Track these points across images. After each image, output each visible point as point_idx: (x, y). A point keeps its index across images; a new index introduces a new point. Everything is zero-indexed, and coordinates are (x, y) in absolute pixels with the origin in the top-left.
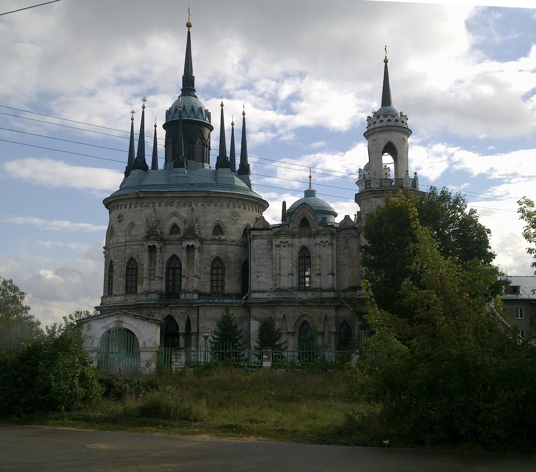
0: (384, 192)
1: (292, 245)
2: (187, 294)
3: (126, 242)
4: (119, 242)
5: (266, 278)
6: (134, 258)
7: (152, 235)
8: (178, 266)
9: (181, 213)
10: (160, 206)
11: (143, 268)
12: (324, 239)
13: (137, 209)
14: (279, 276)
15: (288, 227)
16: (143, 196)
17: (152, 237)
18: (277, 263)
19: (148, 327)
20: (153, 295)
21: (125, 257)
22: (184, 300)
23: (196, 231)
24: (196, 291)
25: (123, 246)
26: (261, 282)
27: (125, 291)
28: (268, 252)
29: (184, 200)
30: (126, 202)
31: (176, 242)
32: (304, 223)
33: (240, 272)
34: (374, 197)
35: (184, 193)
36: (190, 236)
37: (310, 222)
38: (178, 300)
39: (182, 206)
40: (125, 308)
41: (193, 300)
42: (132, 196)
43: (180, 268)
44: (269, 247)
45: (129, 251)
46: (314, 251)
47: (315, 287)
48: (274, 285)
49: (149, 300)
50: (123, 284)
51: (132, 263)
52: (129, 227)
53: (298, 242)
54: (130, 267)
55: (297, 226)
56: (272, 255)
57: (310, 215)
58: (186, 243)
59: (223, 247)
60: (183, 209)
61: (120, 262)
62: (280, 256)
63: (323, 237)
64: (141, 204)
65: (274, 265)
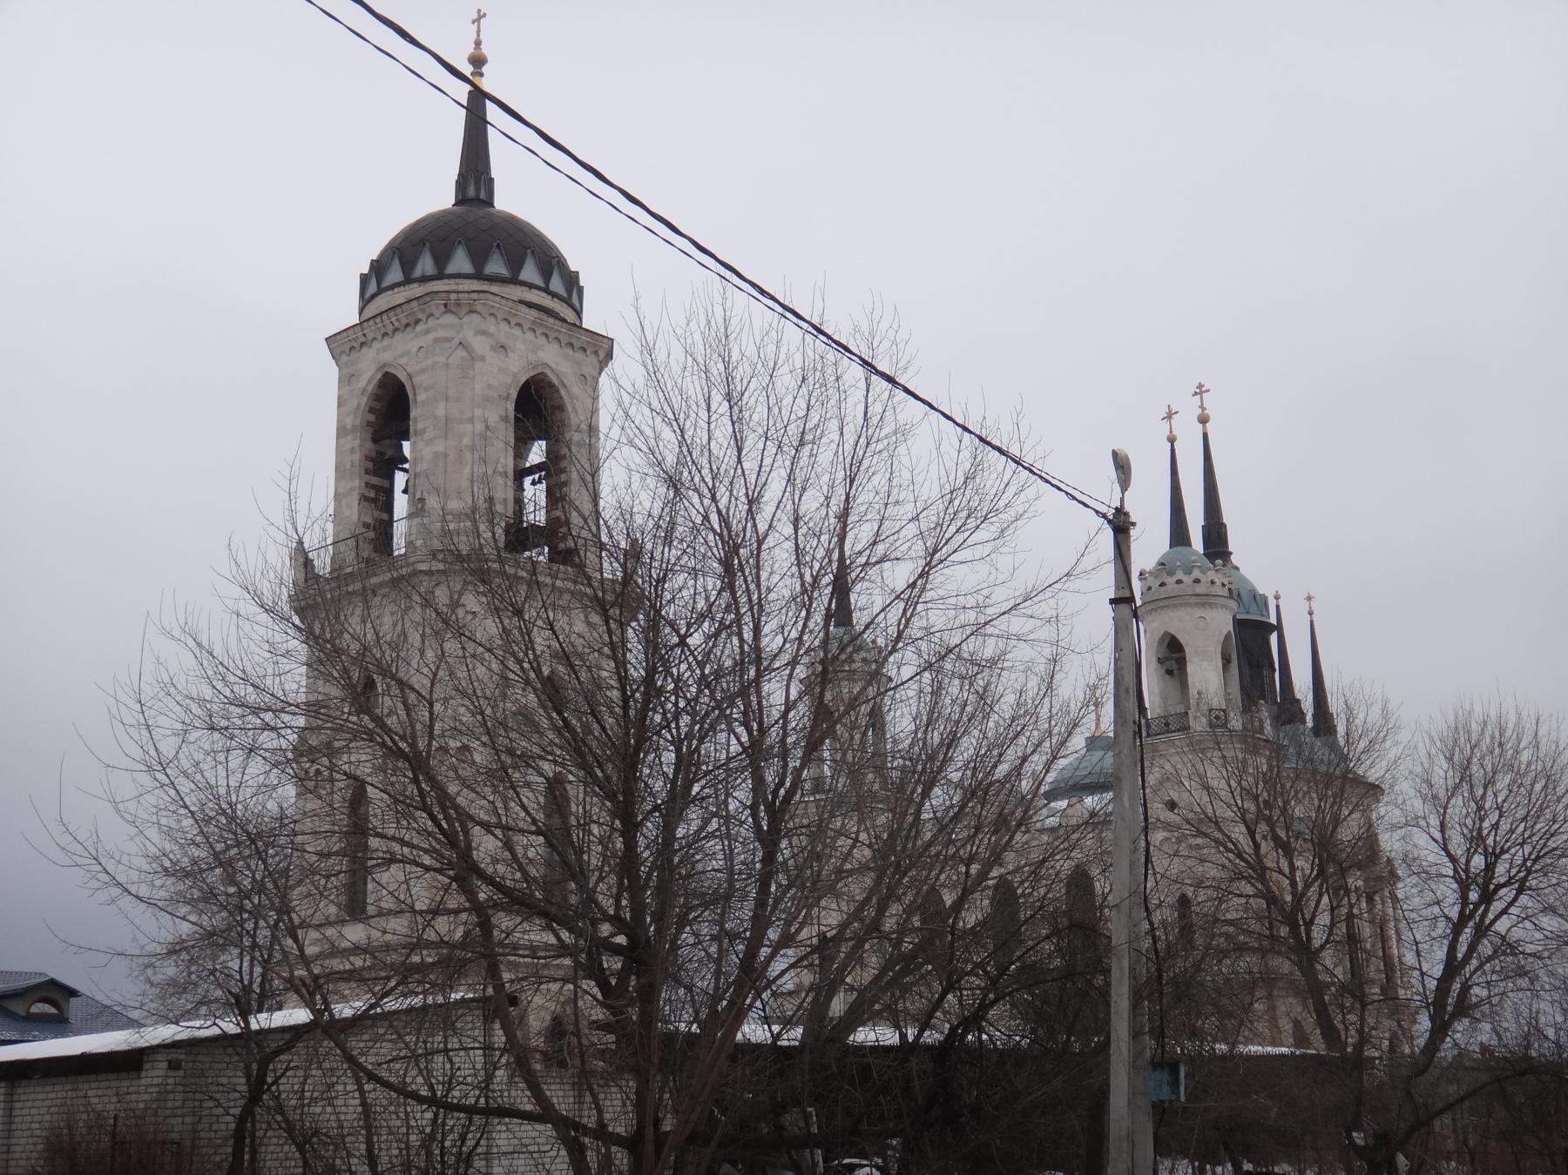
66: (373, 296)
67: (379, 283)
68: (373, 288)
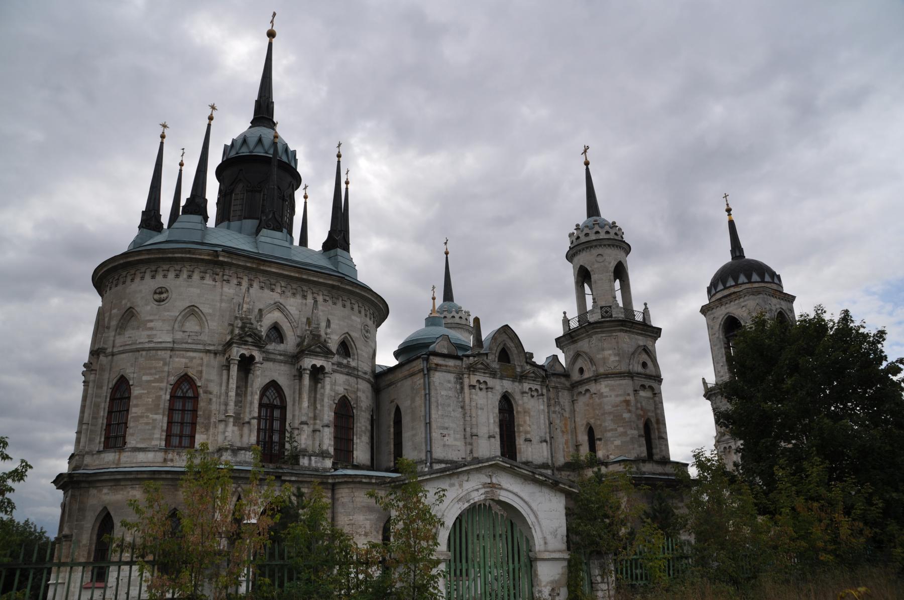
0: (634, 325)
1: (492, 388)
2: (313, 458)
3: (174, 342)
4: (155, 340)
5: (456, 439)
6: (191, 375)
7: (250, 336)
8: (277, 402)
9: (287, 307)
10: (251, 285)
11: (211, 400)
12: (534, 387)
13: (203, 284)
14: (476, 437)
15: (487, 358)
16: (226, 260)
17: (250, 339)
18: (474, 415)
19: (550, 500)
20: (248, 453)
21: (169, 372)
22: (308, 469)
23: (328, 343)
24: (323, 455)
25: (165, 349)
26: (448, 445)
27: (166, 441)
28: (457, 396)
29: (295, 286)
30: (180, 266)
31: (279, 357)
32: (504, 356)
33: (369, 427)
34: (621, 331)
35: (298, 272)
36: (318, 350)
37: (511, 359)
38: (296, 467)
39: (289, 294)
40: (169, 476)
41: (325, 470)
42: (202, 257)
43: (283, 408)
44: (458, 387)
45: (179, 363)
46: (520, 402)
47: (524, 460)
48: (468, 452)
49: (240, 463)
50: (162, 426)
51: (185, 387)
52: (183, 313)
53: (501, 386)
54: (179, 394)
55: (497, 359)
56: (464, 401)
57: (512, 345)
58: (311, 361)
59: (352, 380)
60: (292, 301)
61: (156, 381)
62: (477, 404)
63: (532, 382)
64: (215, 276)
65: (468, 419)
66: (714, 294)
67: (715, 289)
68: (713, 292)
